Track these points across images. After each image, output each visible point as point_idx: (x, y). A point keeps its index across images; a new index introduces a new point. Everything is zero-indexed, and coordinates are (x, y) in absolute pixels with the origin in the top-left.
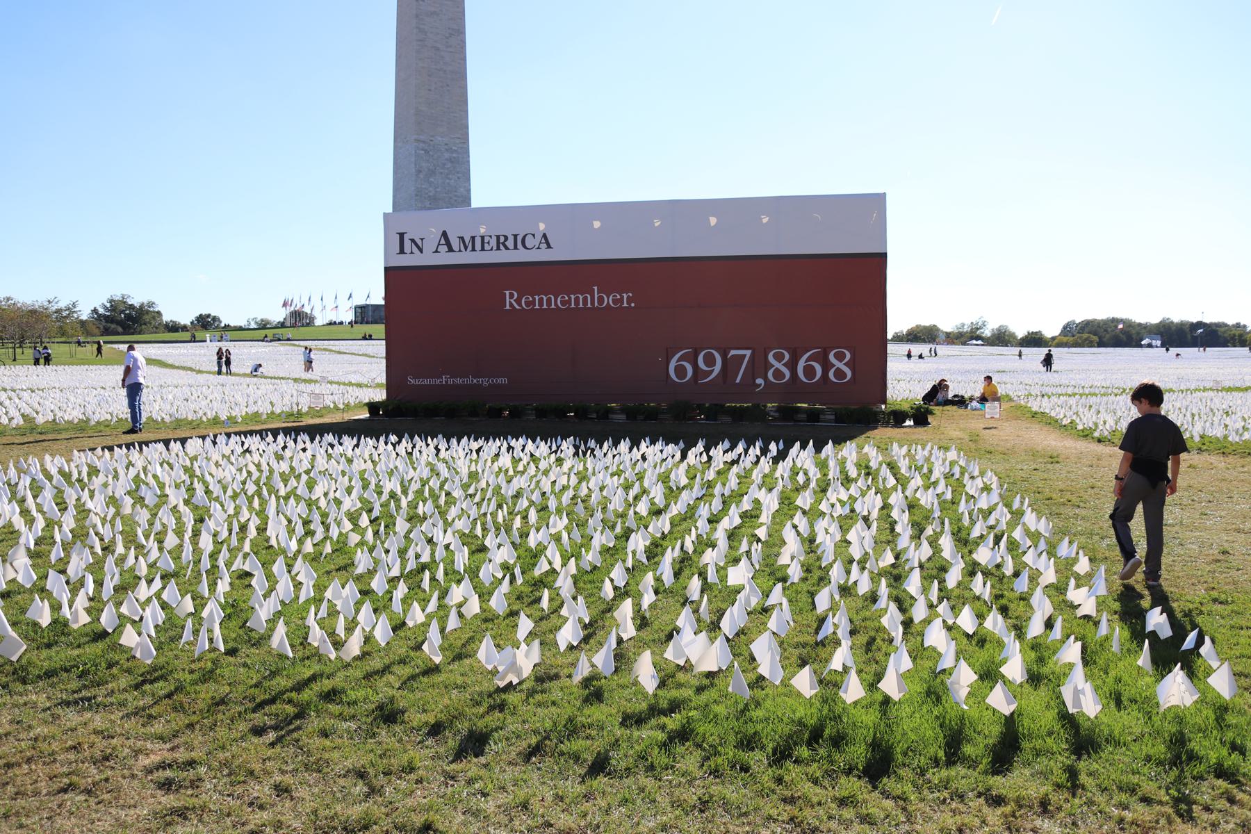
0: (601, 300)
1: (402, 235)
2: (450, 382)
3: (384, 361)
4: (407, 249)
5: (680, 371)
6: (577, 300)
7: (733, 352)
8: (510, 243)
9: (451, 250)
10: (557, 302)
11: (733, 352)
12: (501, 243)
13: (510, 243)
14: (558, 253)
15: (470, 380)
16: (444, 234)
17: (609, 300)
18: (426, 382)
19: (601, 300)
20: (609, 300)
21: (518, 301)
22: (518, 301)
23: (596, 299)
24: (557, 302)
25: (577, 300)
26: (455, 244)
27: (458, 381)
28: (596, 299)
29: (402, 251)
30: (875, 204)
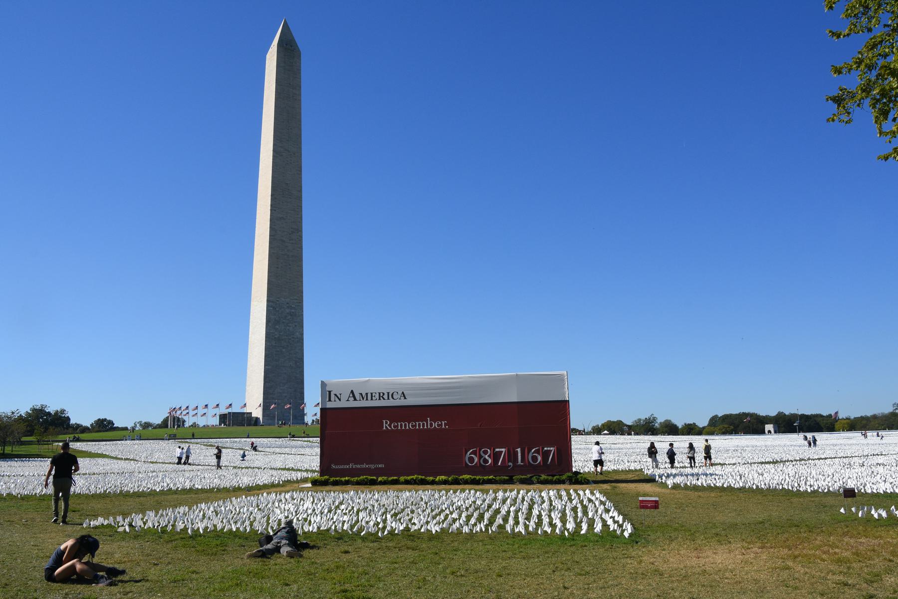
0: (431, 425)
1: (330, 392)
2: (354, 467)
3: (319, 457)
4: (332, 399)
5: (471, 460)
6: (420, 425)
7: (497, 450)
8: (386, 397)
9: (355, 399)
10: (409, 426)
11: (497, 450)
12: (381, 396)
13: (386, 397)
14: (411, 401)
15: (364, 466)
16: (352, 392)
17: (435, 425)
18: (341, 467)
19: (431, 425)
20: (435, 425)
21: (390, 426)
22: (390, 426)
23: (430, 424)
24: (409, 426)
25: (420, 425)
26: (358, 398)
27: (358, 466)
28: (430, 424)
29: (330, 400)
30: (558, 380)
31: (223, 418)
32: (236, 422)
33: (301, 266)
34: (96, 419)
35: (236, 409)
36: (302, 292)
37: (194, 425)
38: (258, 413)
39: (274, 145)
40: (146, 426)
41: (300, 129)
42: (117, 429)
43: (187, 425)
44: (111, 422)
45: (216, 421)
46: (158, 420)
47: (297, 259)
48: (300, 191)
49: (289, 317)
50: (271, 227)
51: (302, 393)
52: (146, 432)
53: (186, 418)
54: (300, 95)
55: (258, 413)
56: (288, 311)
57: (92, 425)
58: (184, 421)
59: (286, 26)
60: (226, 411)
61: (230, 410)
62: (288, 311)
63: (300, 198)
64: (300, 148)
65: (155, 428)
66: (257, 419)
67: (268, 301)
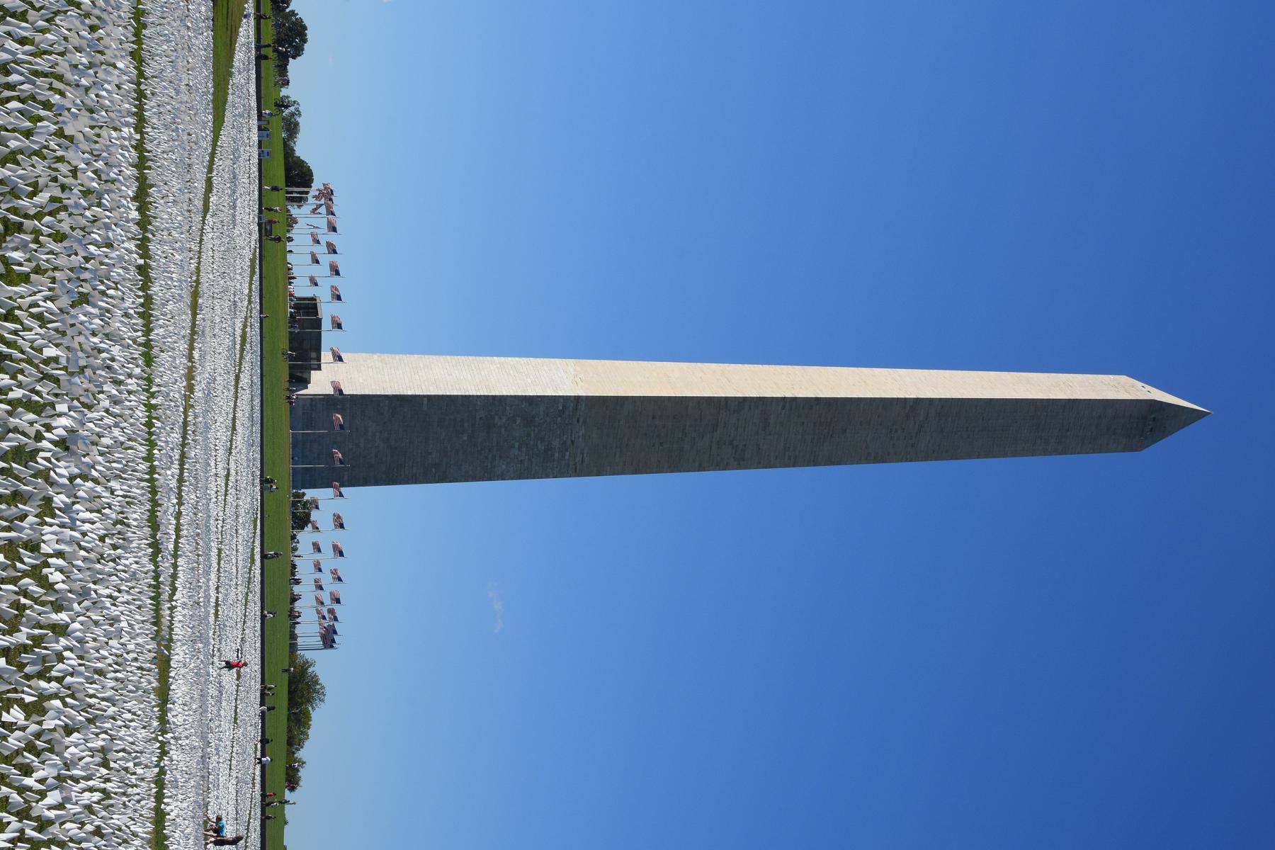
31: (308, 307)
32: (296, 335)
33: (659, 469)
34: (306, 22)
35: (329, 338)
36: (598, 474)
37: (291, 222)
38: (320, 383)
39: (931, 401)
40: (292, 128)
41: (969, 456)
42: (282, 69)
43: (294, 211)
44: (298, 52)
45: (301, 289)
46: (303, 149)
47: (674, 462)
48: (830, 462)
49: (541, 447)
50: (745, 399)
51: (365, 482)
52: (278, 121)
53: (306, 209)
54: (1046, 452)
55: (320, 383)
56: (556, 443)
57: (293, 13)
58: (300, 200)
59: (1203, 414)
60: (326, 311)
61: (326, 324)
62: (556, 443)
63: (814, 461)
64: (926, 458)
65: (285, 144)
66: (305, 382)
67: (578, 398)
